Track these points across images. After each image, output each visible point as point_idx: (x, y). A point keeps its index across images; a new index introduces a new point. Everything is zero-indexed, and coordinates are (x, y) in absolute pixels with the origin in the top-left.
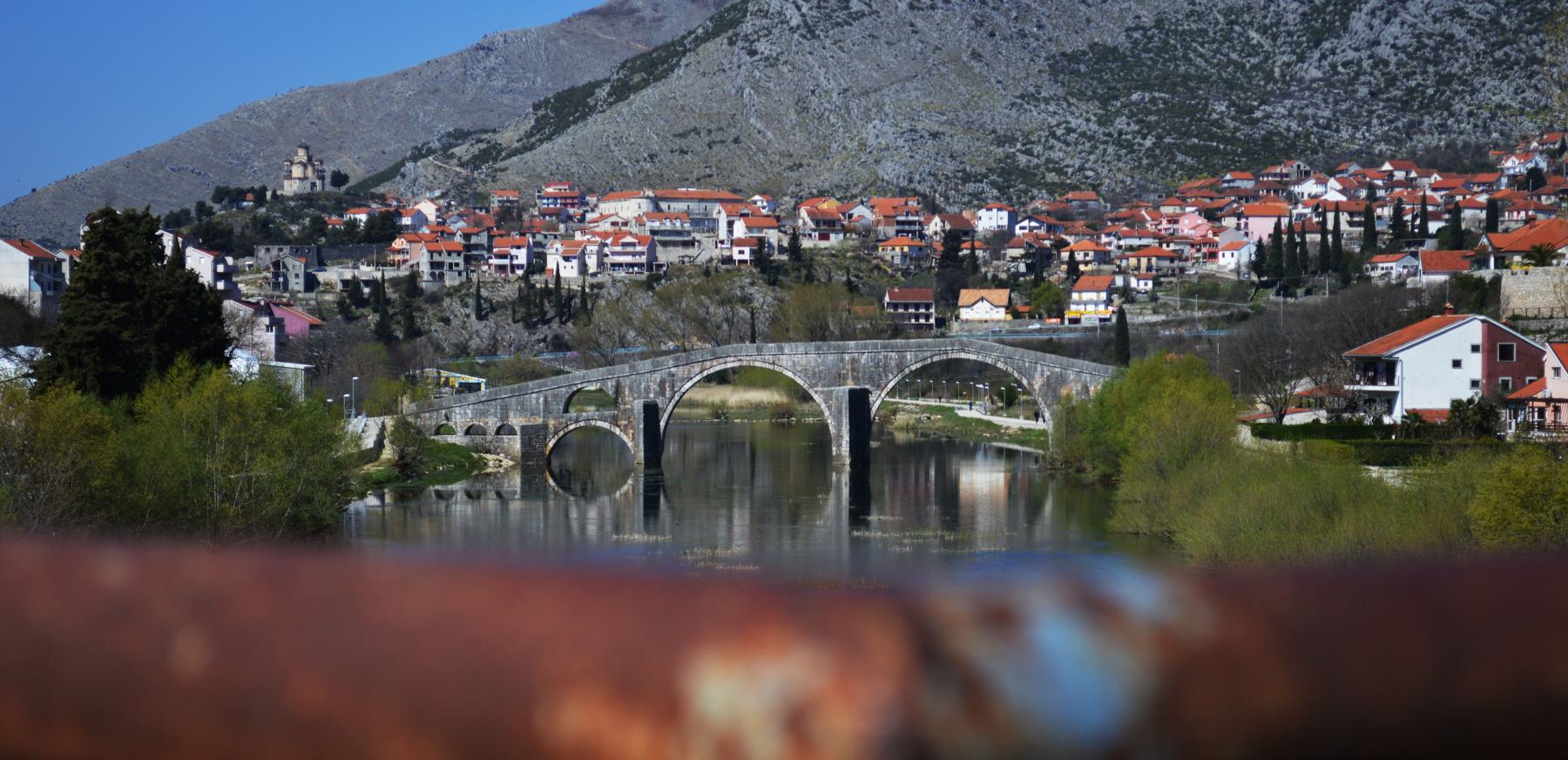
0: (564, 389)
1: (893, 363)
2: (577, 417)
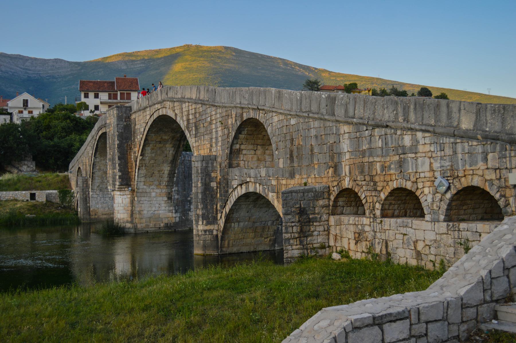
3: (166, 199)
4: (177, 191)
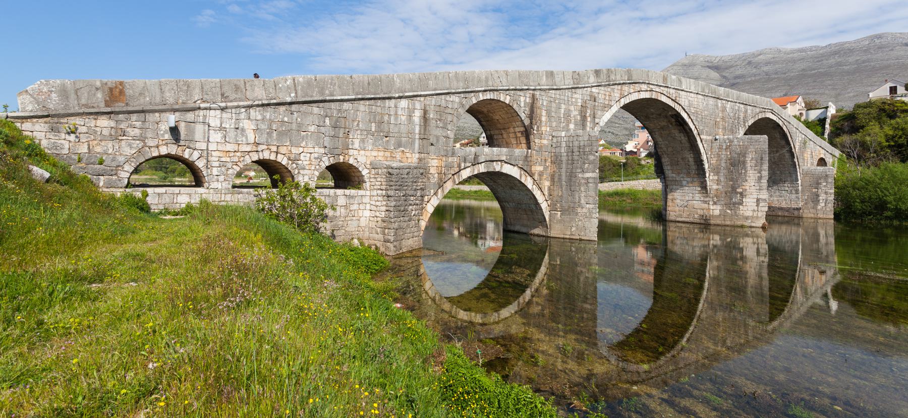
0: (456, 98)
1: (742, 115)
2: (476, 156)
3: (699, 189)
4: (717, 180)
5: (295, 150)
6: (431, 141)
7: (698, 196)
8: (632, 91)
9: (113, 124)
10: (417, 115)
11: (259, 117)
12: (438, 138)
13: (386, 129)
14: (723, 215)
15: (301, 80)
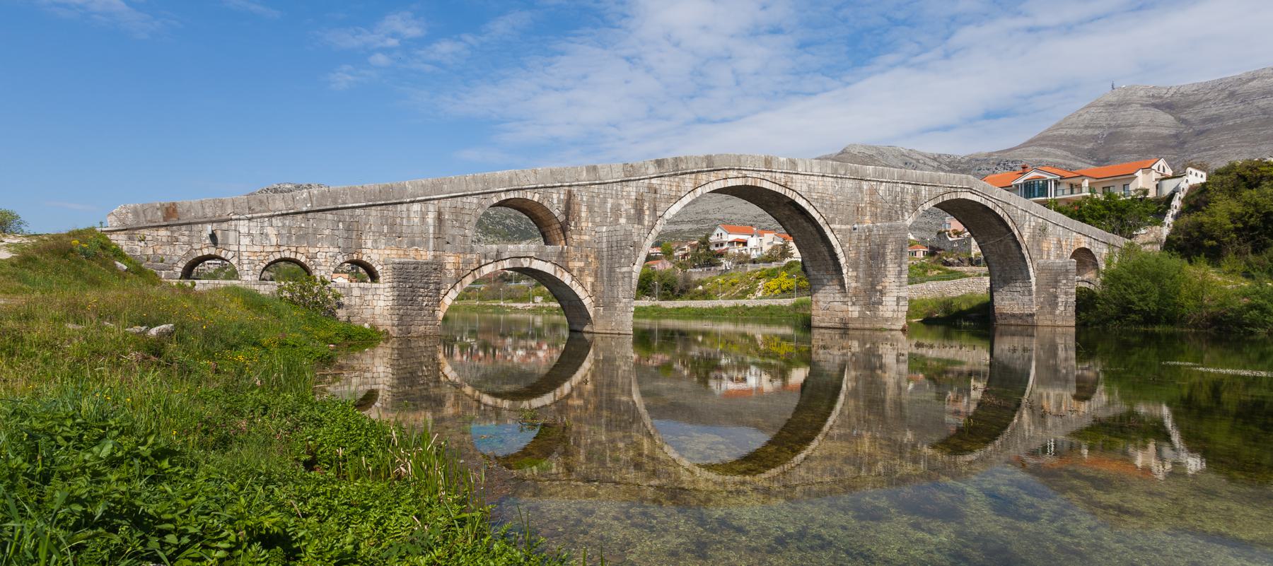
0: (474, 200)
1: (909, 198)
2: (498, 252)
3: (839, 288)
4: (856, 277)
5: (312, 250)
6: (447, 240)
7: (838, 297)
8: (713, 179)
9: (169, 233)
10: (431, 218)
11: (280, 224)
12: (454, 237)
13: (399, 230)
14: (862, 316)
15: (316, 192)
